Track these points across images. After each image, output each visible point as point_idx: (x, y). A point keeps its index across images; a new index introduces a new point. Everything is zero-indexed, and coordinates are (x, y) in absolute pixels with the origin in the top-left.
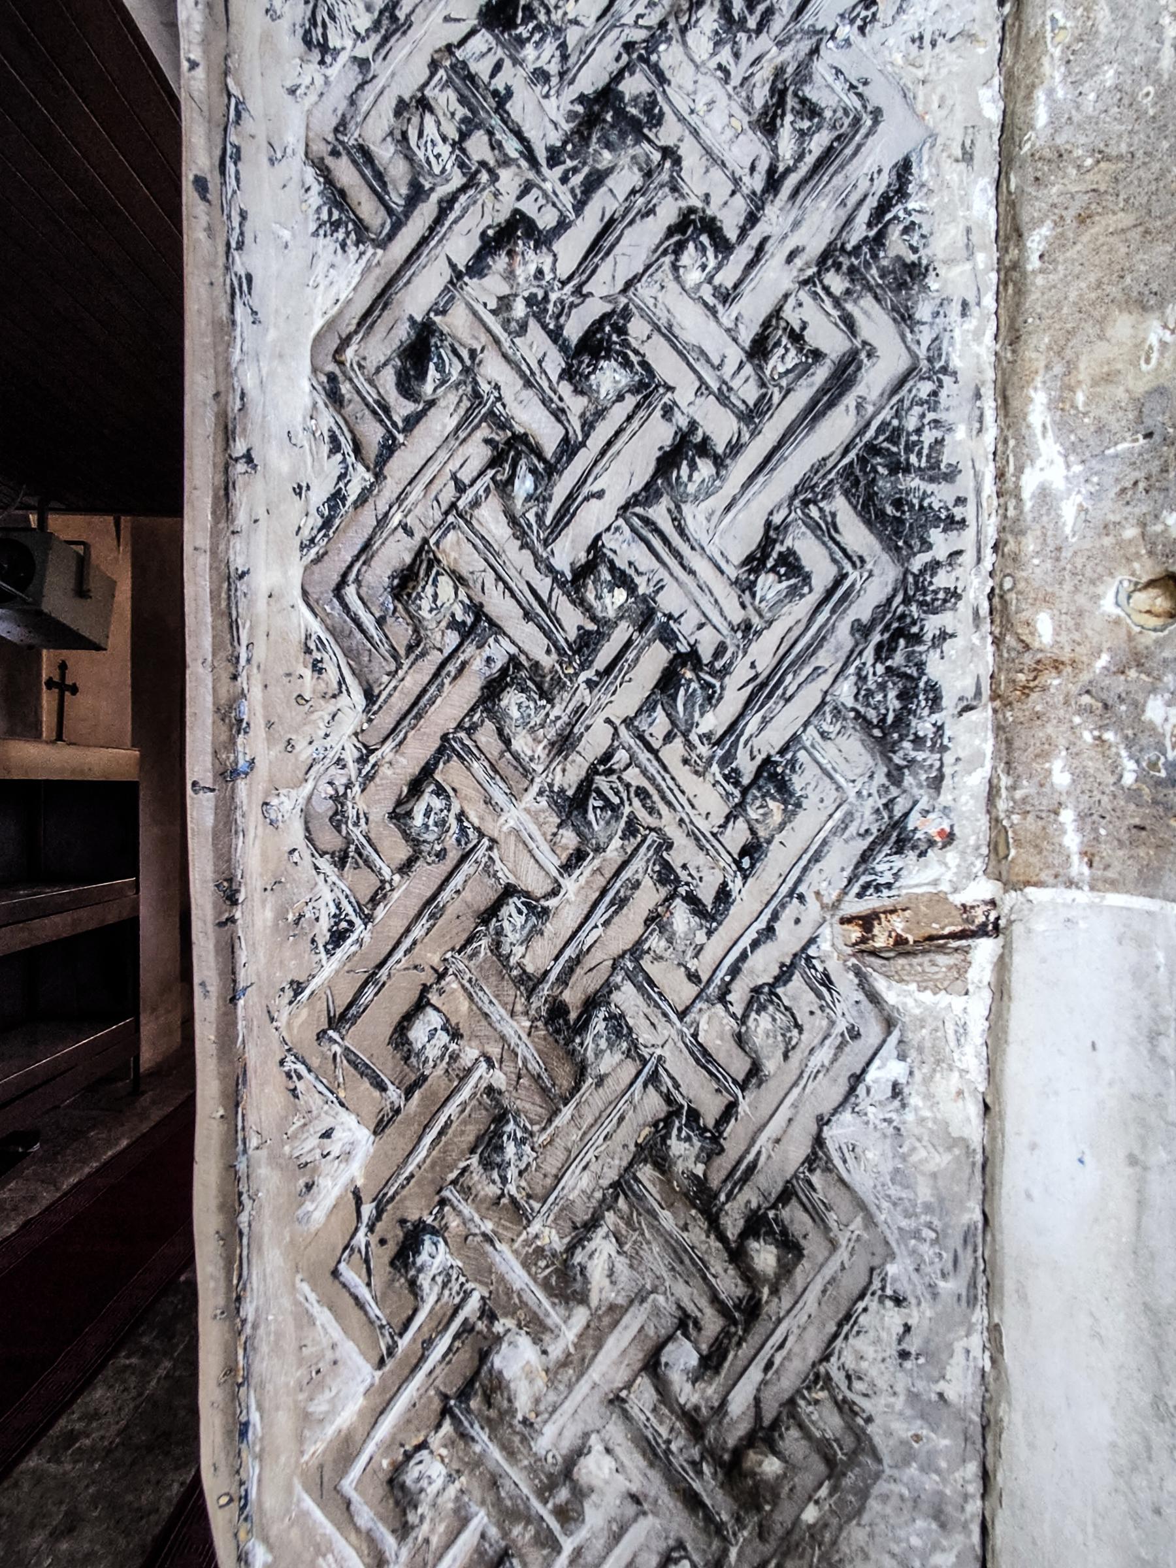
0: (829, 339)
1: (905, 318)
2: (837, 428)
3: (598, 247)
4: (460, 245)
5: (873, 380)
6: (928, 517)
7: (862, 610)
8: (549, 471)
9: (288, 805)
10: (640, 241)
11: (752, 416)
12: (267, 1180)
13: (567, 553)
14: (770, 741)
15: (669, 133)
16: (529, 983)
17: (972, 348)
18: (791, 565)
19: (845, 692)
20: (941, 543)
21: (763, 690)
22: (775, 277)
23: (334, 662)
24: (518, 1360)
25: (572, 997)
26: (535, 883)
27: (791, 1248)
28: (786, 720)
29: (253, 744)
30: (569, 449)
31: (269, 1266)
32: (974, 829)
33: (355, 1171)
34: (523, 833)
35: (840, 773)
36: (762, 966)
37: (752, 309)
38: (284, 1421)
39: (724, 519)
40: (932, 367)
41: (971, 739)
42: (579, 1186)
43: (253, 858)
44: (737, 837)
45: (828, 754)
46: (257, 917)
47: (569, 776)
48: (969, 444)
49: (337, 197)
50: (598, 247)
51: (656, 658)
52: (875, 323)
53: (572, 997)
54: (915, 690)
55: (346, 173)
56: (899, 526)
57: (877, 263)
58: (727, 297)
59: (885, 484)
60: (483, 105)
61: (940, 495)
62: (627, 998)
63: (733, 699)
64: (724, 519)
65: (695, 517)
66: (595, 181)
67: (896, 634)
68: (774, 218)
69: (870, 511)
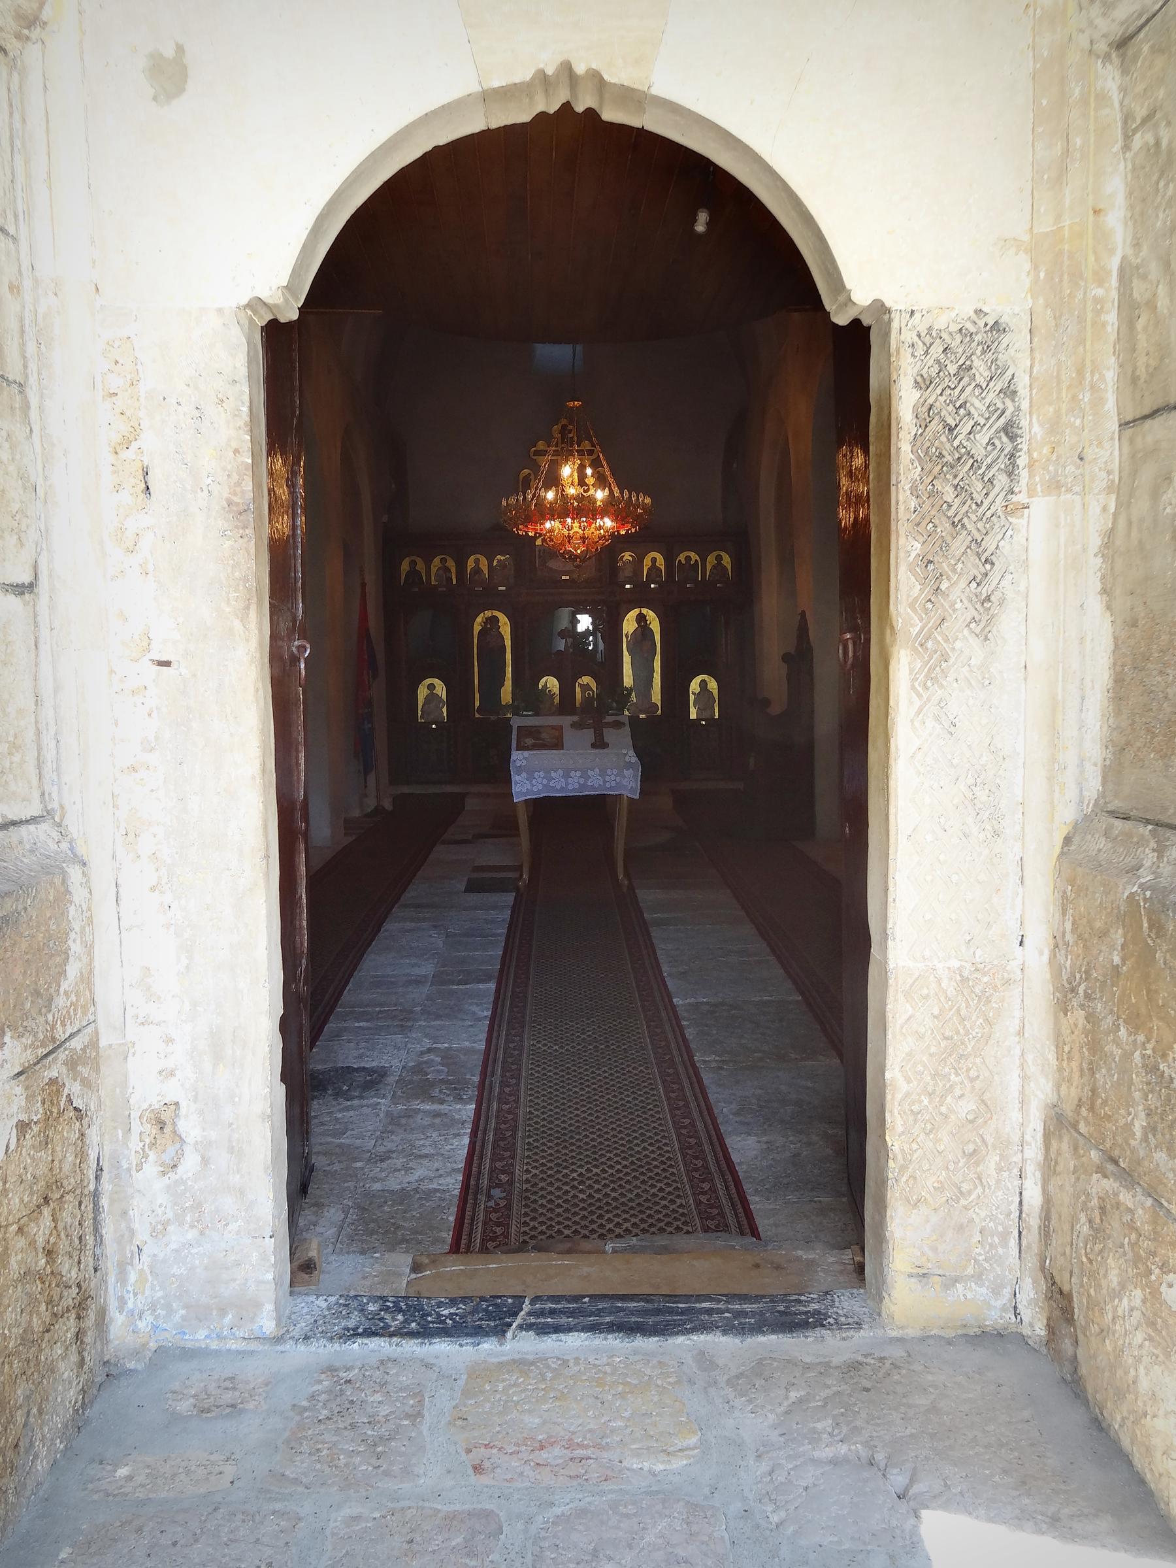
0: (1000, 405)
1: (1013, 401)
2: (1002, 421)
3: (962, 391)
4: (939, 391)
5: (1008, 413)
6: (1017, 436)
7: (1006, 452)
8: (951, 430)
9: (907, 487)
10: (969, 389)
11: (988, 419)
12: (902, 554)
13: (956, 443)
14: (991, 475)
15: (974, 371)
16: (949, 518)
17: (1025, 405)
18: (993, 444)
19: (1003, 466)
20: (1019, 440)
21: (989, 467)
22: (992, 395)
23: (916, 463)
24: (943, 587)
25: (956, 520)
26: (950, 500)
27: (993, 564)
28: (993, 471)
29: (902, 478)
30: (956, 426)
31: (903, 568)
32: (1024, 490)
33: (918, 551)
34: (949, 494)
35: (1002, 480)
36: (989, 514)
37: (988, 401)
38: (904, 597)
39: (983, 438)
40: (1018, 409)
41: (1024, 474)
42: (958, 553)
43: (901, 498)
44: (985, 491)
45: (1000, 477)
46: (902, 508)
47: (956, 482)
48: (1024, 423)
49: (916, 382)
50: (962, 391)
51: (971, 461)
52: (1008, 402)
53: (956, 520)
54: (1014, 465)
55: (919, 379)
56: (1013, 438)
57: (1010, 392)
58: (983, 399)
59: (1010, 431)
60: (942, 367)
61: (1019, 432)
62: (965, 520)
63: (984, 468)
64: (983, 438)
65: (977, 436)
66: (961, 379)
67: (1012, 456)
68: (992, 384)
69: (1007, 434)
